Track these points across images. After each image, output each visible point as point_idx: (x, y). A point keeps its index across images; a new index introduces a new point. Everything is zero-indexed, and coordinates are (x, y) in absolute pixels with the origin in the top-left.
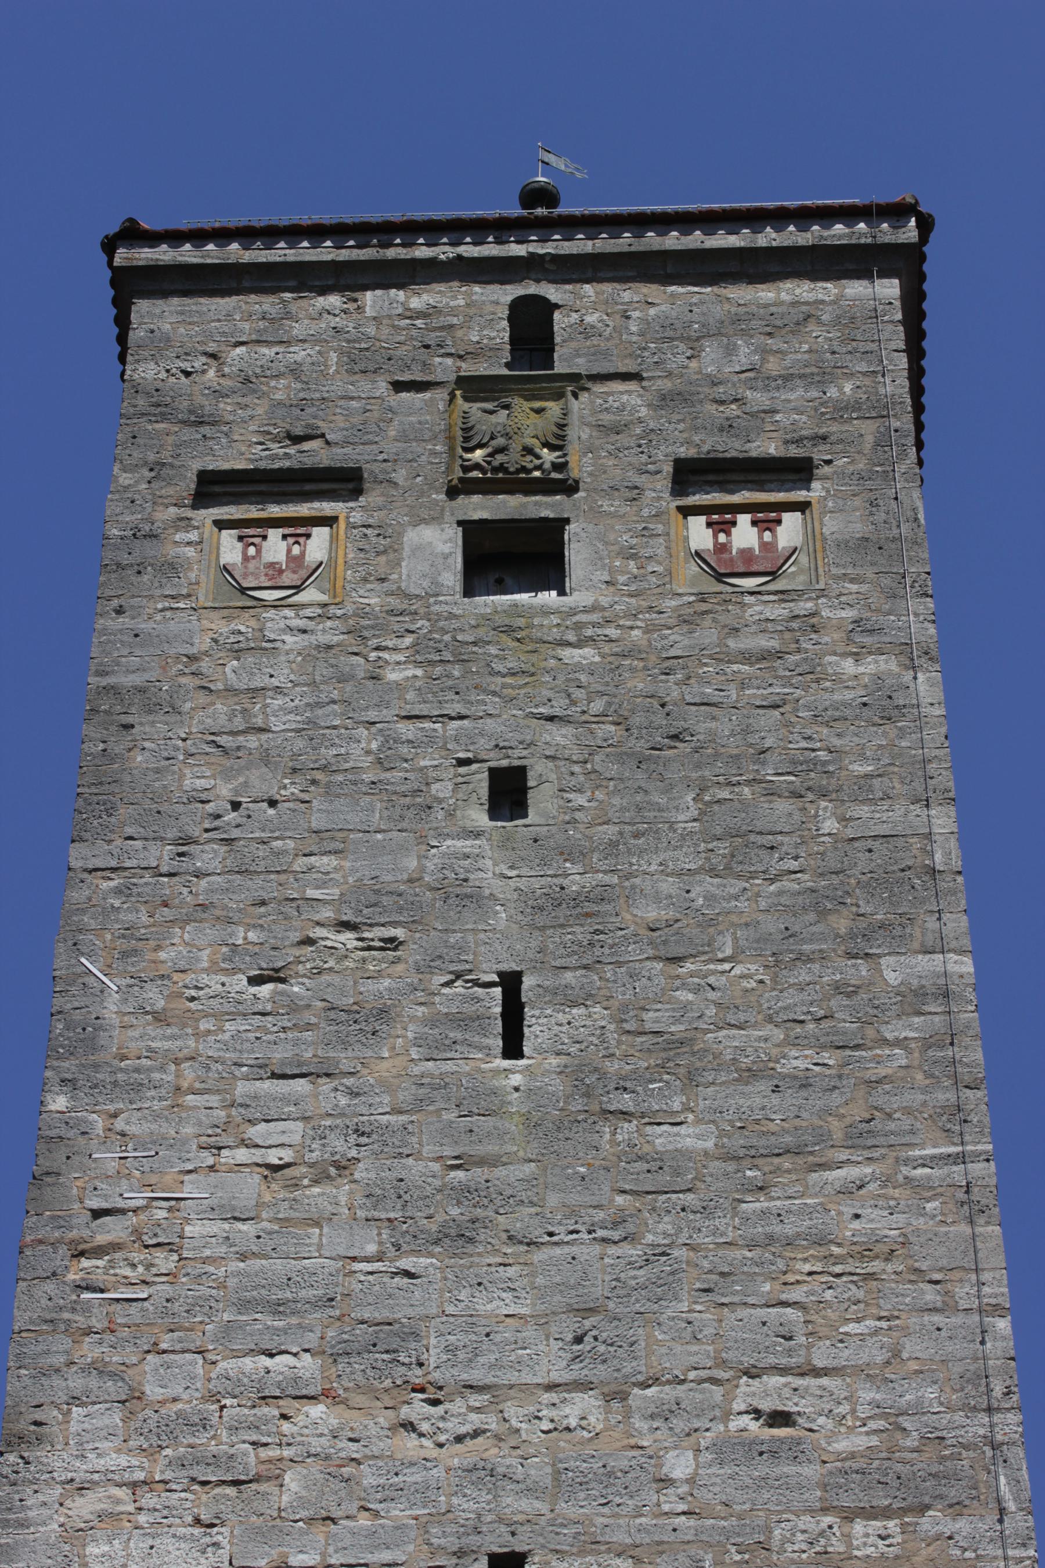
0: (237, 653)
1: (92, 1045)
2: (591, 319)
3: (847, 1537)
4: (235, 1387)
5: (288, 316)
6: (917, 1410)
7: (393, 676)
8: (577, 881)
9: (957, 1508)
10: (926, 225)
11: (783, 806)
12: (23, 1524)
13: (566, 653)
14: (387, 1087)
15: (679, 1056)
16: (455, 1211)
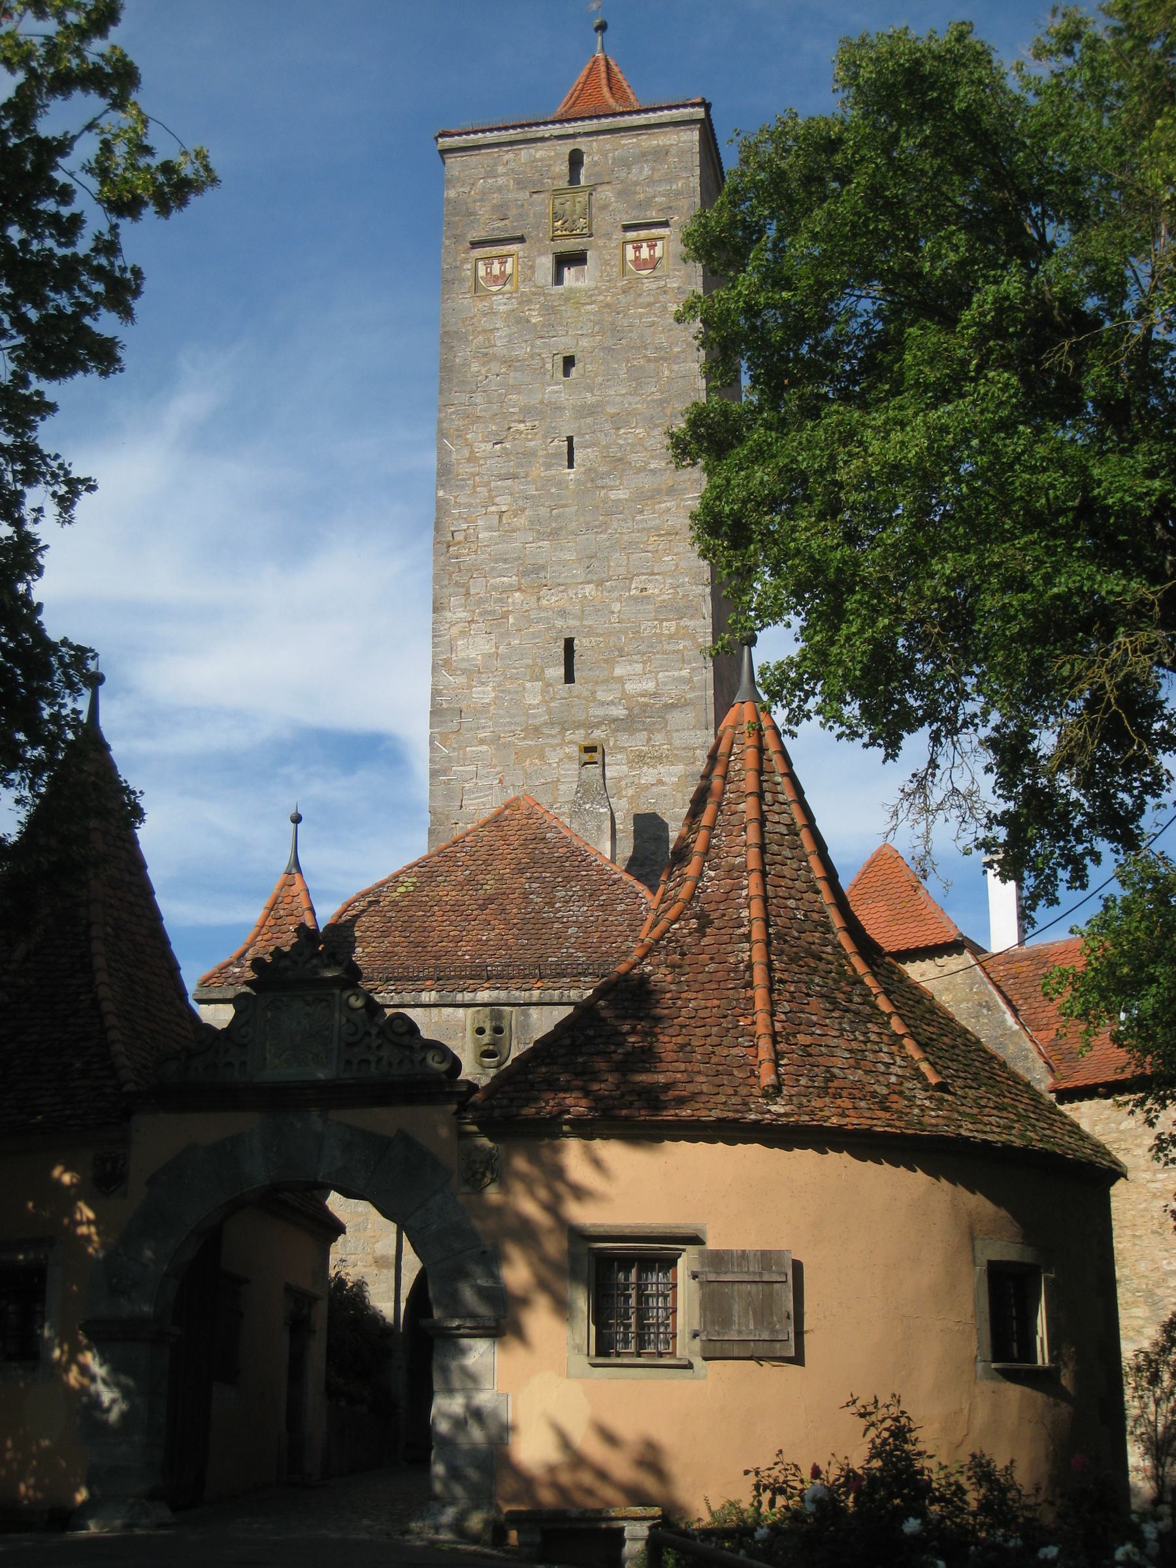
0: (485, 315)
1: (449, 472)
2: (596, 158)
3: (661, 629)
4: (495, 588)
5: (496, 165)
6: (683, 585)
7: (534, 321)
8: (590, 399)
9: (692, 617)
10: (707, 106)
11: (652, 365)
12: (440, 636)
13: (588, 307)
14: (534, 482)
15: (618, 464)
16: (554, 525)
